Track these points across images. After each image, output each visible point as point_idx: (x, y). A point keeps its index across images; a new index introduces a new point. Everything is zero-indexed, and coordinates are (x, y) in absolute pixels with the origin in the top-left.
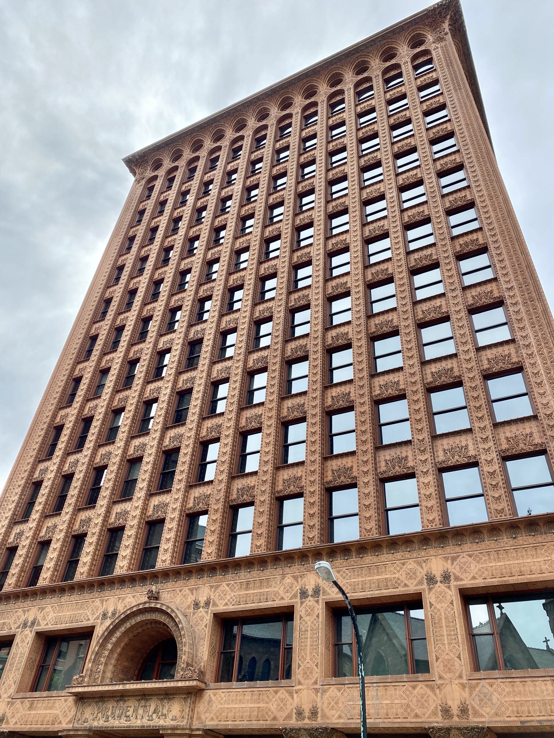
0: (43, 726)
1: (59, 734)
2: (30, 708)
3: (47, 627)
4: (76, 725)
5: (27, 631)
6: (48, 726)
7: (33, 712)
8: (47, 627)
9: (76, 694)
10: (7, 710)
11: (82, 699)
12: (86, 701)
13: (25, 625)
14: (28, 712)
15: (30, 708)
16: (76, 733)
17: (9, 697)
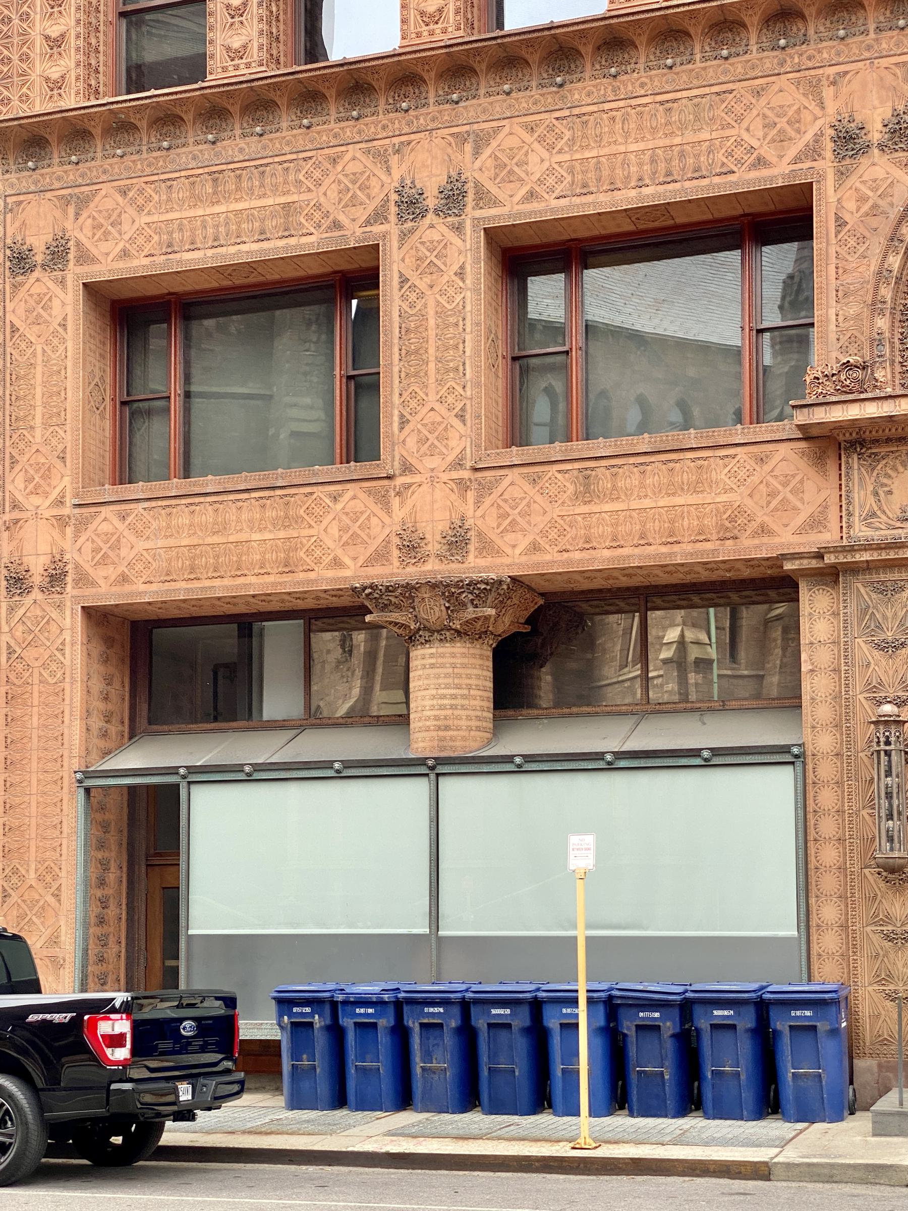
0: (676, 548)
1: (788, 566)
2: (587, 491)
3: (536, 206)
4: (861, 532)
5: (434, 229)
6: (708, 546)
7: (607, 507)
8: (536, 206)
9: (808, 434)
10: (469, 509)
11: (836, 446)
12: (883, 450)
13: (411, 206)
14: (585, 509)
15: (587, 491)
16: (892, 555)
17: (458, 464)
